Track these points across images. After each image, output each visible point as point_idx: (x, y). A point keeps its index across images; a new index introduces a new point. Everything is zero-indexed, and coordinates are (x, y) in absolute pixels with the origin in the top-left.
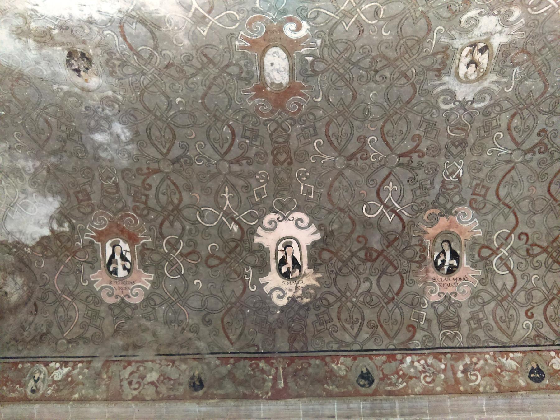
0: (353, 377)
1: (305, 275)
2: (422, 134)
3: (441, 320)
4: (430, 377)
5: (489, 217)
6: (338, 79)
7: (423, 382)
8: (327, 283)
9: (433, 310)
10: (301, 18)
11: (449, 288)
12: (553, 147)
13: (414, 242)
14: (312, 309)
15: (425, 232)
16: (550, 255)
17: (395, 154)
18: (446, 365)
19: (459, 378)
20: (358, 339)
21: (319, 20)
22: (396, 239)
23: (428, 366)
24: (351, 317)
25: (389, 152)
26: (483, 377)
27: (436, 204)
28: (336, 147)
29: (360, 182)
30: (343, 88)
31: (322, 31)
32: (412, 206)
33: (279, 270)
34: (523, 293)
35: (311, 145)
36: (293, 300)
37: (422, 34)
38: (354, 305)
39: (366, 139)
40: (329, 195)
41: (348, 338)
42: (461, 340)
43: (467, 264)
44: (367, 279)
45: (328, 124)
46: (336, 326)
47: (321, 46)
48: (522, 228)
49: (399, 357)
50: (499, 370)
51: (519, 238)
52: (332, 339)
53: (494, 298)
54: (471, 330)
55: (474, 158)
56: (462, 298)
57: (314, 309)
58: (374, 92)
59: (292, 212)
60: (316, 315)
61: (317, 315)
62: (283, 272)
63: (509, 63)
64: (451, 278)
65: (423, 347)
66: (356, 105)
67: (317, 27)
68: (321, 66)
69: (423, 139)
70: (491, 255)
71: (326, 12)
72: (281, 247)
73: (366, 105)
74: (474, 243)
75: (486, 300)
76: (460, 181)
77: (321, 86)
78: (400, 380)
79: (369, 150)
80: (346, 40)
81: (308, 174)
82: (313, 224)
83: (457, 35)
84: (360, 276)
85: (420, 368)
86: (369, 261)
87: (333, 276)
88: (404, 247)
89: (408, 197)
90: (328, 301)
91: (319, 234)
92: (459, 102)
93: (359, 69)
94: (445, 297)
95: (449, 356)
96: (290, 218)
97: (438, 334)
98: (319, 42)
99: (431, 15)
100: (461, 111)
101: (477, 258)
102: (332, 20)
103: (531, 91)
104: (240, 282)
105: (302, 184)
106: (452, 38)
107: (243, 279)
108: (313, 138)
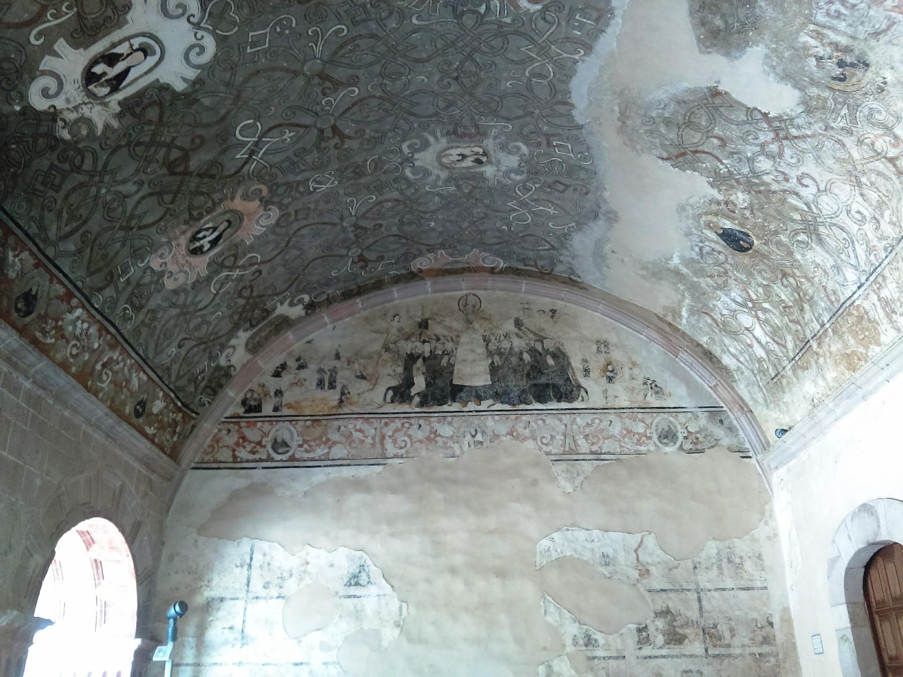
0: (18, 290)
1: (106, 105)
2: (367, 136)
3: (136, 291)
4: (78, 348)
5: (271, 237)
6: (449, 42)
7: (68, 350)
8: (109, 142)
9: (141, 274)
10: (547, 4)
11: (175, 266)
12: (363, 239)
13: (216, 196)
14: (57, 152)
15: (232, 199)
16: (244, 307)
17: (336, 121)
18: (100, 345)
19: (95, 369)
20: (60, 244)
21: (541, 24)
22: (213, 177)
23: (87, 333)
24: (78, 208)
25: (336, 115)
26: (111, 382)
27: (274, 187)
28: (337, 53)
29: (287, 101)
30: (434, 47)
31: (523, 25)
32: (266, 167)
33: (95, 62)
34: (200, 320)
35: (337, 22)
36: (53, 115)
37: (503, 113)
38: (97, 197)
39: (355, 85)
40: (258, 72)
41: (52, 233)
42: (127, 328)
43: (210, 258)
44: (141, 184)
45: (372, 36)
46: (56, 202)
47: (500, 22)
48: (265, 268)
49: (74, 302)
50: (124, 384)
51: (254, 274)
52: (38, 217)
53: (184, 306)
54: (143, 322)
55: (341, 192)
56: (169, 284)
57: (58, 157)
58: (426, 80)
59: (213, 33)
60: (52, 164)
61: (52, 167)
62: (93, 70)
63: (460, 182)
64: (187, 258)
65: (100, 309)
66: (405, 64)
67: (531, 20)
68: (469, 21)
69: (360, 140)
70: (226, 267)
71: (551, 31)
72: (136, 43)
73: (407, 74)
74: (236, 246)
75: (178, 303)
76: (311, 193)
77: (438, 22)
78: (53, 332)
79: (337, 93)
80: (507, 48)
81: (287, 32)
82: (199, 71)
83: (498, 141)
84: (141, 173)
85: (78, 332)
86: (168, 170)
87: (123, 143)
88: (205, 190)
89: (277, 158)
90: (83, 162)
91: (185, 85)
92: (413, 156)
93: (461, 62)
94: (162, 271)
95: (109, 337)
96: (200, 33)
97: (122, 305)
98: (508, 20)
99: (528, 119)
100: (399, 160)
101: (220, 260)
102: (538, 35)
103: (426, 204)
104: (35, 8)
105: (268, 30)
106: (495, 138)
107: (44, 8)
108: (349, 22)
